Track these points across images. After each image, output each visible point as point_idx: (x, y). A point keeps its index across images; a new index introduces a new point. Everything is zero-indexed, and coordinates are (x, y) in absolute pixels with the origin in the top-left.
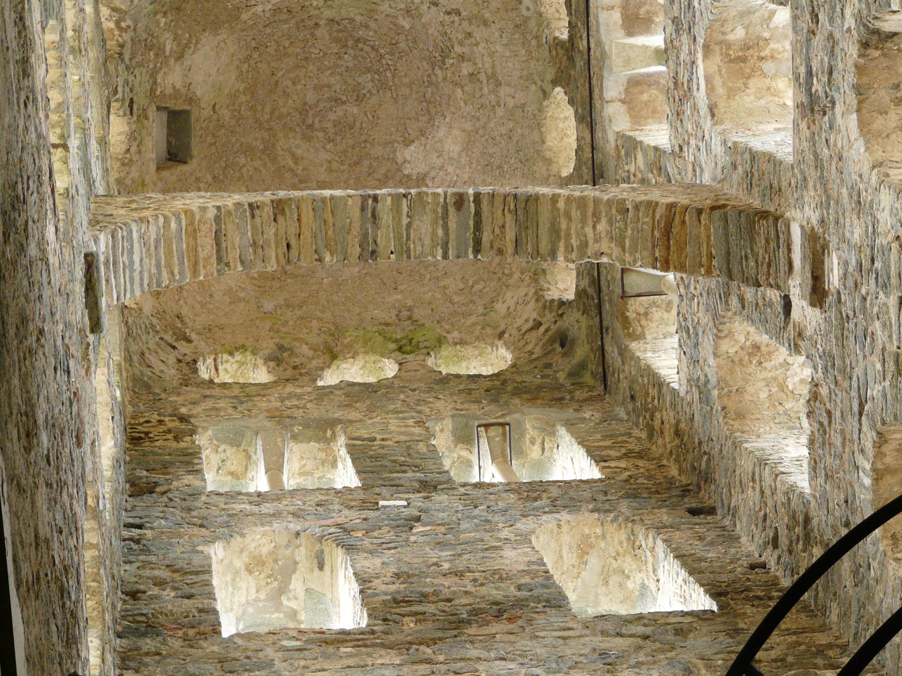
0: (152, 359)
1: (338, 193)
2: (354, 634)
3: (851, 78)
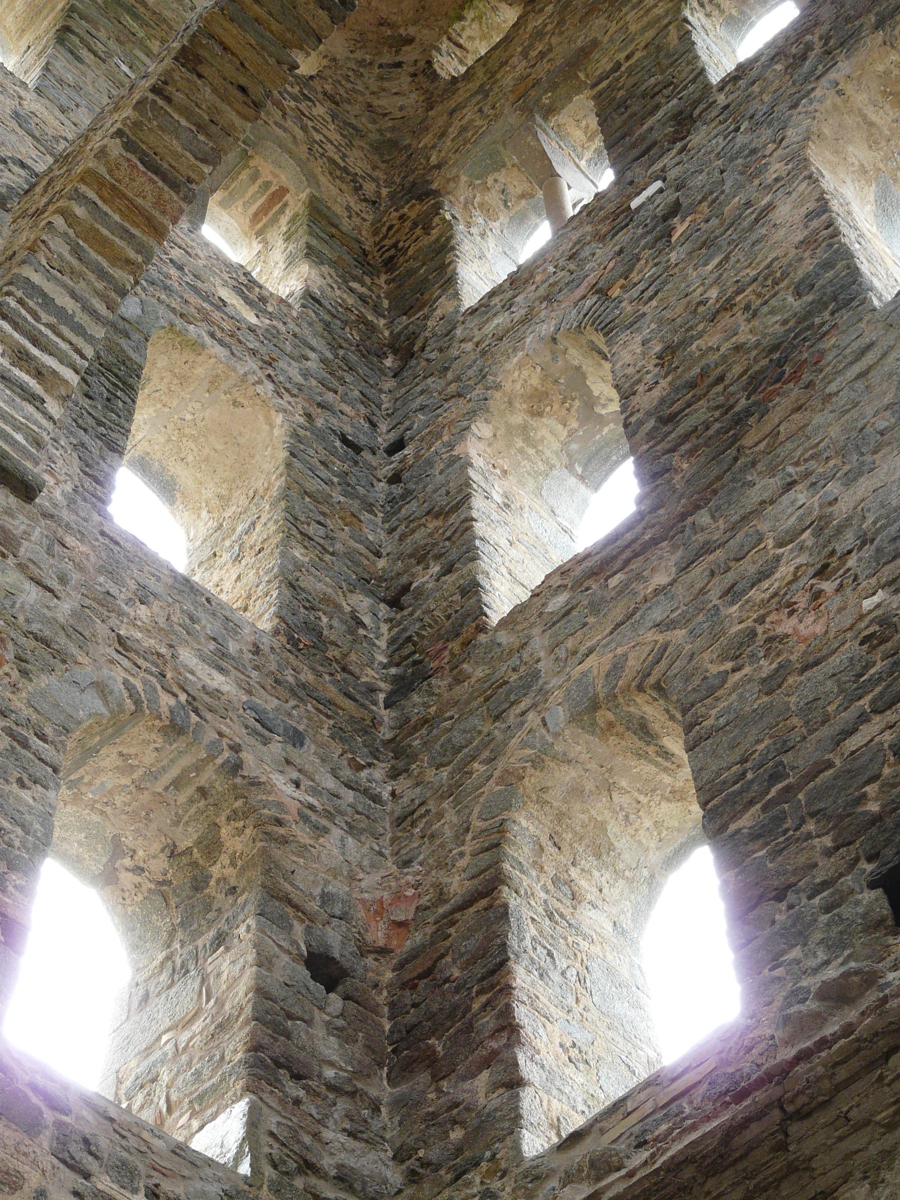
0: (382, 102)
2: (623, 534)
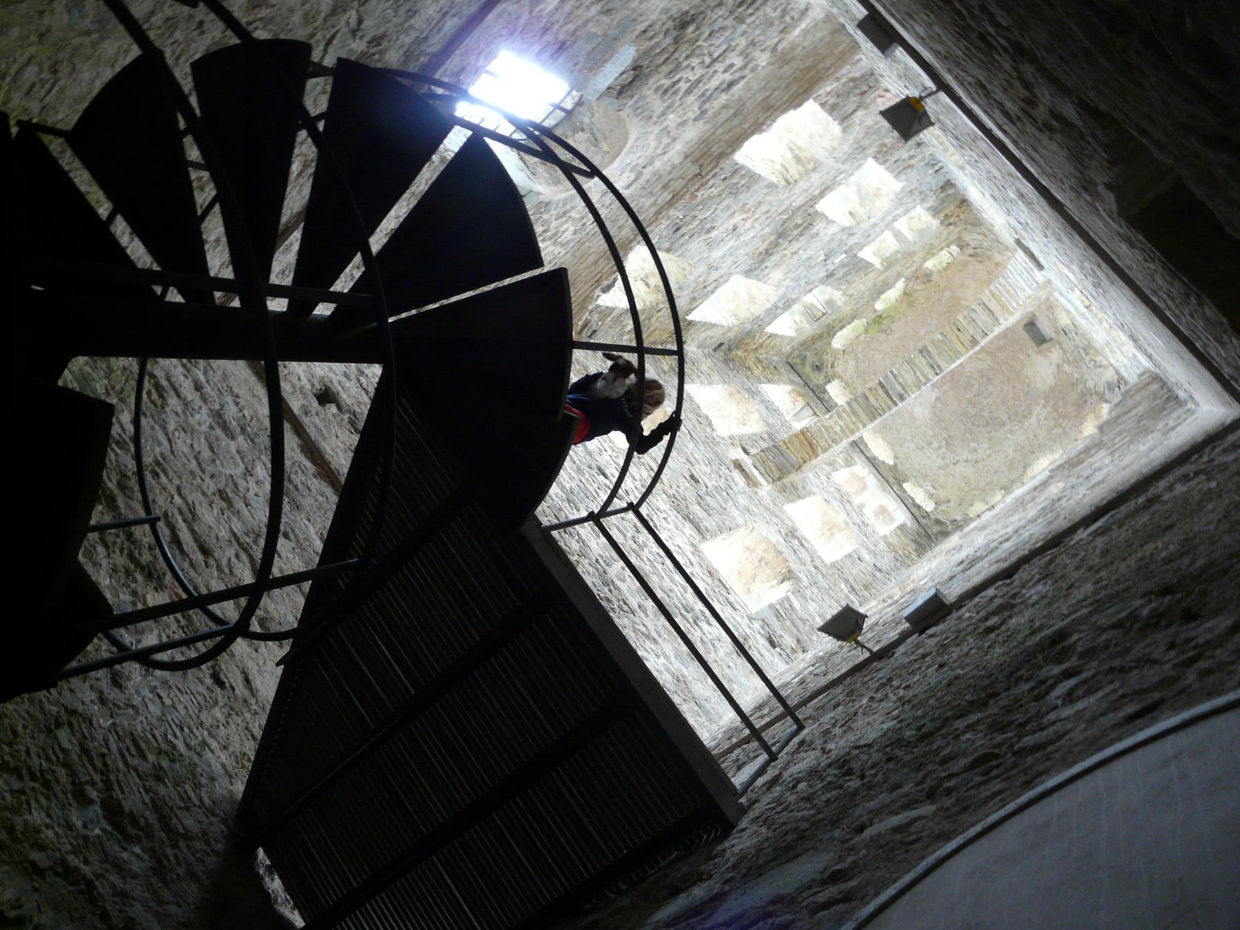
0: (979, 237)
1: (954, 366)
3: (786, 555)
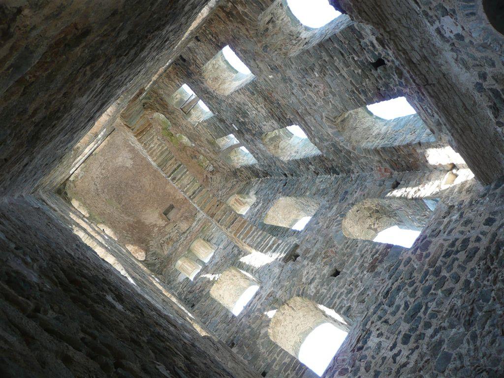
0: (218, 181)
